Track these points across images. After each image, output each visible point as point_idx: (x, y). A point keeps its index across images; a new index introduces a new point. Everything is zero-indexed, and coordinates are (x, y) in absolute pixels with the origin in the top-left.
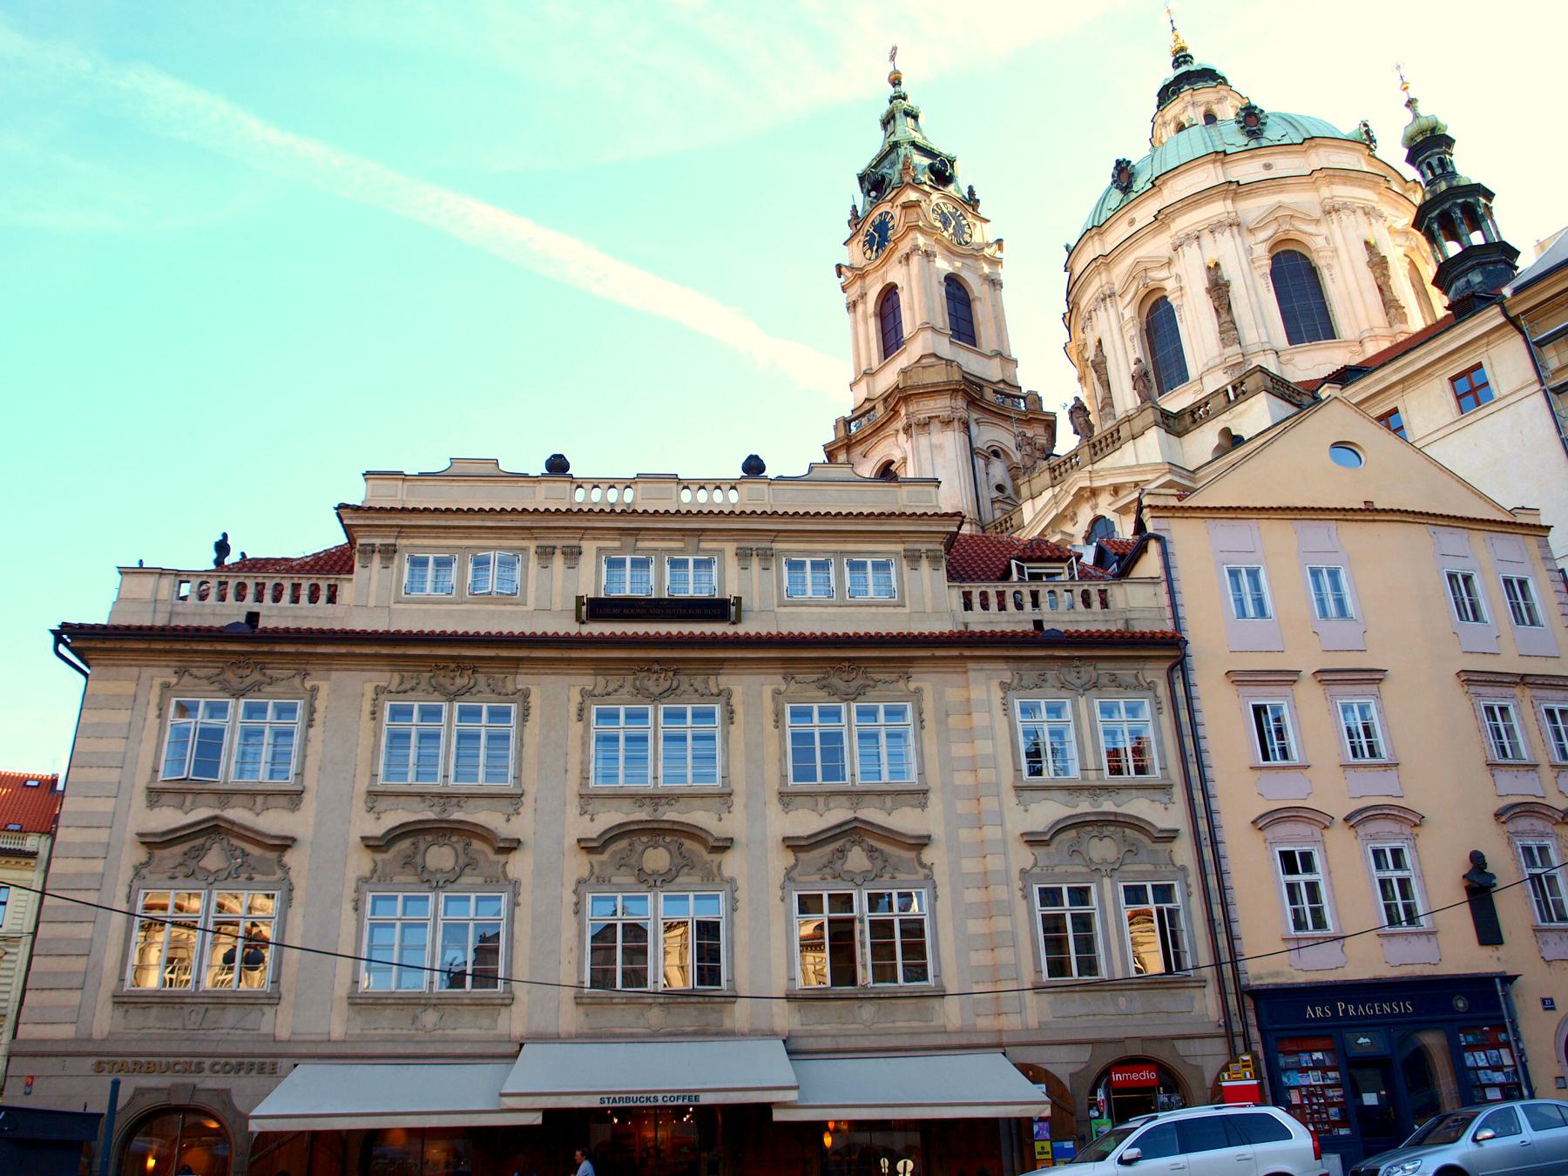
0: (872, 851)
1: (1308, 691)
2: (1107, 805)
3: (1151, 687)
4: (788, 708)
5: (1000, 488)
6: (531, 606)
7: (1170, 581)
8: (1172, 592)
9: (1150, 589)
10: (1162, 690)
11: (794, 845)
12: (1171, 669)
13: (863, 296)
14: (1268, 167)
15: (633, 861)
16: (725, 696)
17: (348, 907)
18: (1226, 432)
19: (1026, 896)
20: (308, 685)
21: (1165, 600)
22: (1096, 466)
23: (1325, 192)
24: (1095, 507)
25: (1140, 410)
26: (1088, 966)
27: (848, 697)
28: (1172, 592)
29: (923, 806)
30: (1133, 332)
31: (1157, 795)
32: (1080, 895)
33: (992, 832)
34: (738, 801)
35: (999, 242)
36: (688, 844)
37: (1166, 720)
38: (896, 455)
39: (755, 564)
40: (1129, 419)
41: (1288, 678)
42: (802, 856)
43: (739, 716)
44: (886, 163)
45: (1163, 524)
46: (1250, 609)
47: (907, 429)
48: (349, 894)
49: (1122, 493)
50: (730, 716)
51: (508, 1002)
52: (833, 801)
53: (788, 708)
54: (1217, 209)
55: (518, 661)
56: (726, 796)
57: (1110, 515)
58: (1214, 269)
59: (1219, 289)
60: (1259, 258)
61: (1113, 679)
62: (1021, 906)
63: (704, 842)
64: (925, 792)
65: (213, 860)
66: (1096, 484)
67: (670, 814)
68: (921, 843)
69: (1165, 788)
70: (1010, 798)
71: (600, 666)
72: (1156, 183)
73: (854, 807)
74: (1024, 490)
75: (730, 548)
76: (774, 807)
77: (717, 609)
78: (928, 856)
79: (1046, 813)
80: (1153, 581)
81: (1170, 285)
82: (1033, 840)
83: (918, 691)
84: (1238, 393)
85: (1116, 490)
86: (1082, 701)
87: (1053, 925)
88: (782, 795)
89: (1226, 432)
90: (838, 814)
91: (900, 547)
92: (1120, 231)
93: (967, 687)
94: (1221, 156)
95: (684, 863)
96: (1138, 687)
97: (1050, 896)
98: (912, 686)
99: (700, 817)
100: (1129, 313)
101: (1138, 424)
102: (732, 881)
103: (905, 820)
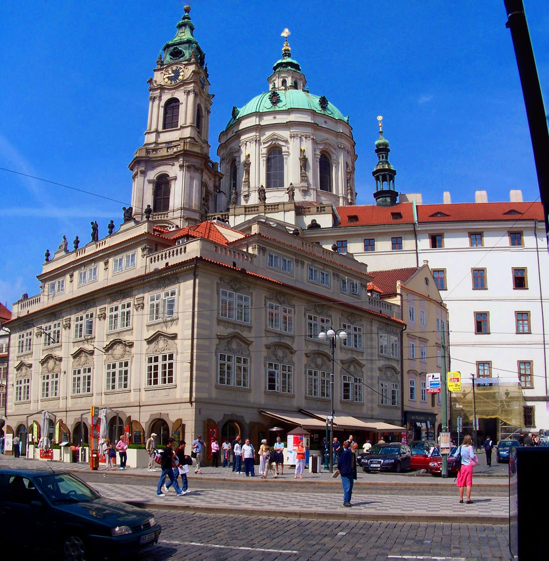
0: (355, 366)
6: (294, 279)
13: (160, 97)
14: (326, 122)
15: (315, 361)
16: (331, 316)
17: (263, 365)
18: (314, 221)
20: (251, 291)
22: (268, 215)
23: (339, 140)
25: (289, 203)
30: (265, 159)
35: (214, 96)
38: (171, 175)
40: (284, 204)
44: (182, 46)
47: (181, 167)
48: (263, 362)
51: (293, 397)
54: (309, 131)
55: (294, 296)
58: (302, 151)
59: (304, 161)
60: (318, 155)
64: (363, 353)
65: (234, 346)
71: (309, 302)
72: (290, 111)
73: (352, 354)
74: (232, 211)
75: (332, 272)
81: (284, 149)
84: (321, 210)
89: (314, 221)
92: (267, 120)
93: (371, 325)
94: (313, 112)
100: (264, 151)
101: (287, 207)
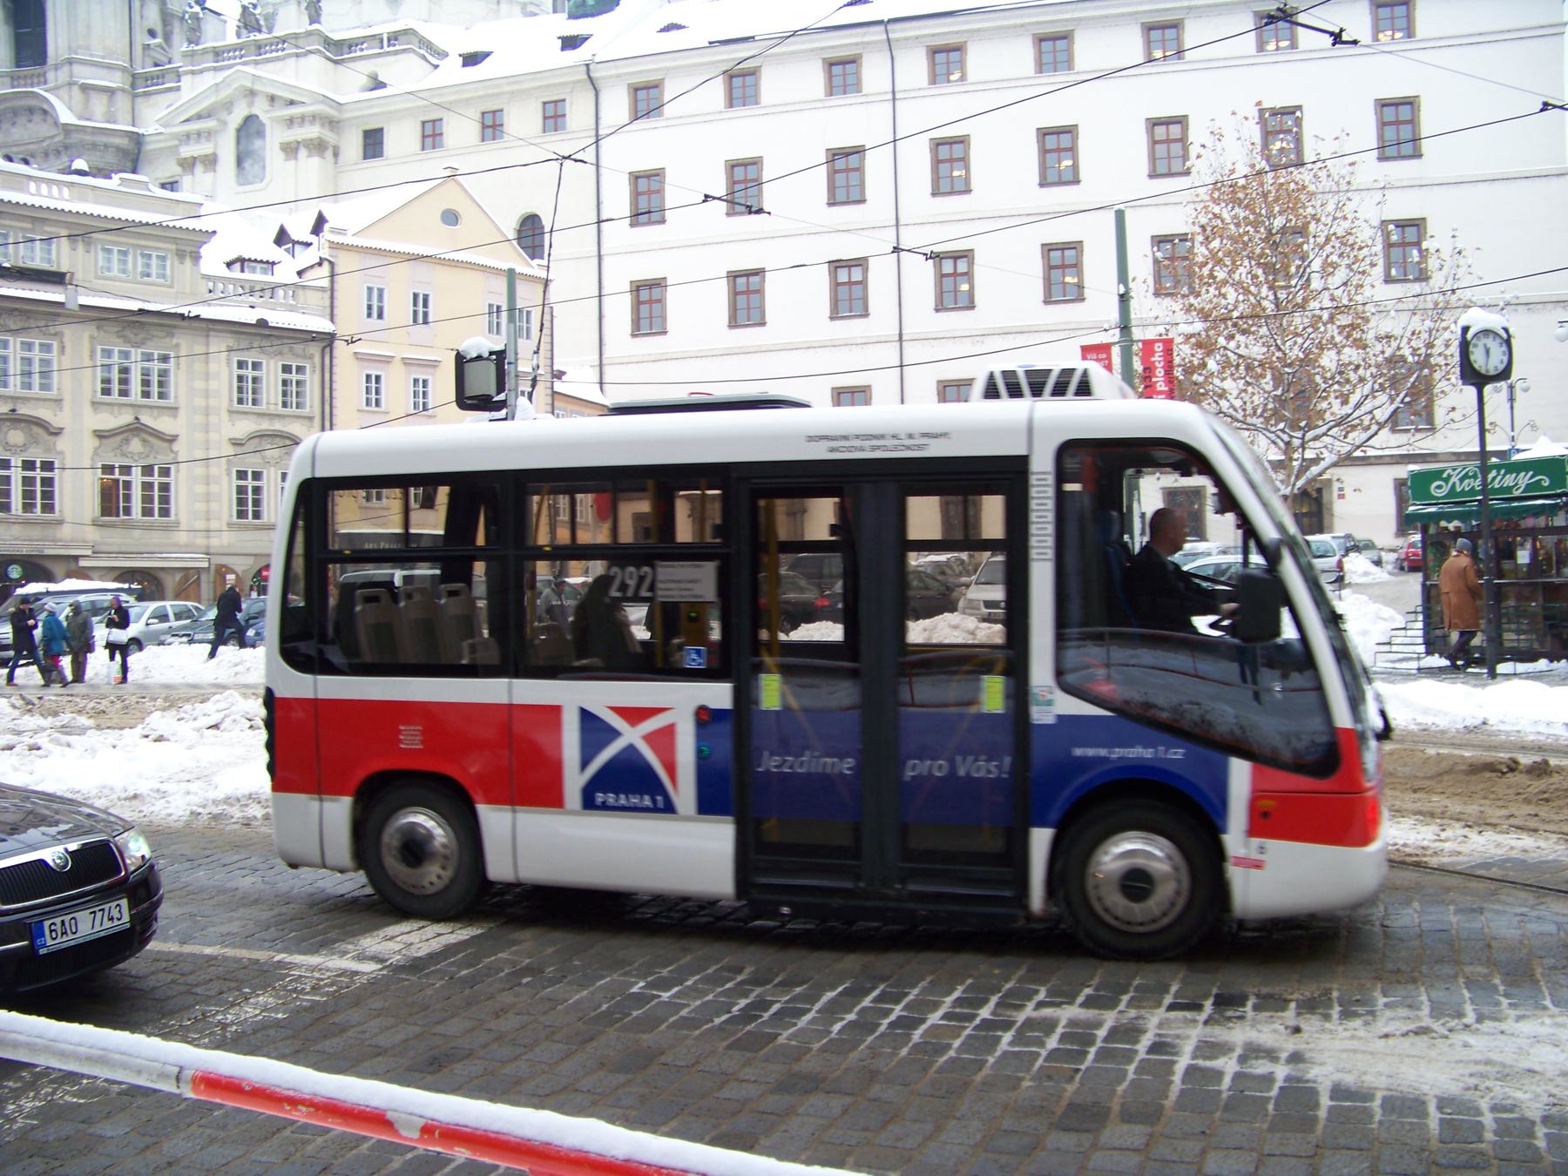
0: (144, 441)
1: (397, 367)
2: (278, 426)
3: (311, 357)
4: (99, 348)
5: (152, 33)
7: (332, 290)
8: (332, 298)
9: (320, 294)
10: (317, 359)
11: (100, 435)
12: (323, 349)
19: (229, 474)
21: (328, 302)
24: (251, 104)
26: (257, 515)
27: (137, 345)
28: (332, 298)
29: (175, 417)
31: (305, 422)
32: (257, 476)
33: (213, 436)
34: (67, 405)
36: (35, 429)
37: (317, 378)
39: (81, 247)
41: (387, 360)
42: (105, 441)
43: (68, 350)
45: (334, 252)
46: (375, 314)
49: (277, 104)
50: (62, 350)
52: (124, 410)
53: (99, 348)
56: (58, 401)
57: (263, 117)
61: (291, 350)
62: (225, 480)
63: (46, 429)
64: (176, 409)
66: (257, 87)
67: (23, 410)
68: (172, 439)
69: (311, 419)
70: (225, 416)
76: (88, 409)
77: (56, 278)
78: (175, 447)
79: (244, 427)
80: (322, 289)
82: (236, 443)
83: (177, 345)
85: (272, 99)
86: (272, 362)
87: (241, 490)
88: (93, 403)
90: (126, 418)
91: (174, 247)
95: (35, 441)
96: (305, 357)
97: (242, 475)
98: (175, 341)
99: (43, 413)
102: (61, 453)
103: (163, 424)
